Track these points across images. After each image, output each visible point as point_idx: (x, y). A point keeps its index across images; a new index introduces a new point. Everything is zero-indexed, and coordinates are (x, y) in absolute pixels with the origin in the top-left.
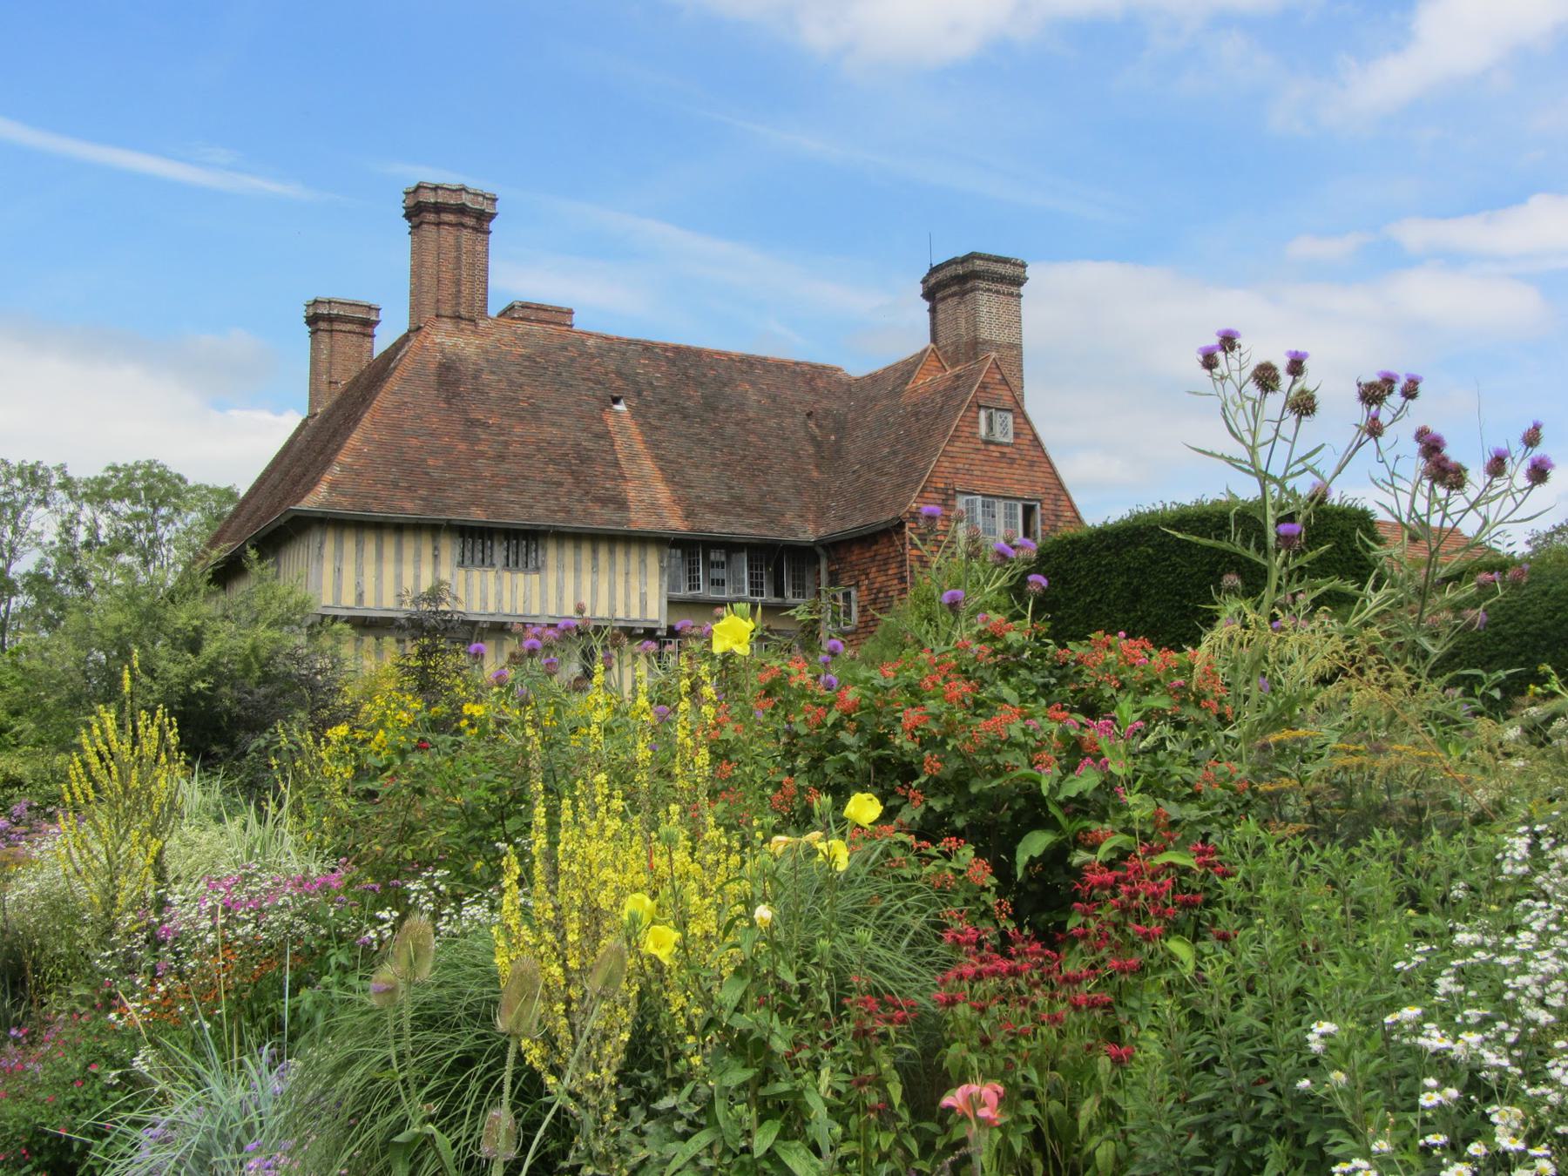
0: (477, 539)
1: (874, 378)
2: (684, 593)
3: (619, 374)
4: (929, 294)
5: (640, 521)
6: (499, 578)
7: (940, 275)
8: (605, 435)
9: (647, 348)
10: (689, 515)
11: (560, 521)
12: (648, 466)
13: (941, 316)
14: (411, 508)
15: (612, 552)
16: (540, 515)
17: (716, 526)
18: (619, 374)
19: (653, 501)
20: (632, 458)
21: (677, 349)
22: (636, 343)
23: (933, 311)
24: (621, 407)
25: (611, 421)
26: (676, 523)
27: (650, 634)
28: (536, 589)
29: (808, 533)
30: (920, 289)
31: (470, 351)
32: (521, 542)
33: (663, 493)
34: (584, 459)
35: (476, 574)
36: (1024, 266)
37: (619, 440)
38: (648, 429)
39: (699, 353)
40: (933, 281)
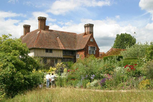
0: (47, 50)
1: (80, 35)
2: (64, 55)
3: (57, 34)
4: (85, 27)
5: (61, 48)
6: (49, 54)
7: (86, 25)
8: (57, 40)
9: (59, 31)
10: (65, 48)
11: (54, 48)
12: (61, 43)
13: (86, 29)
14: (42, 47)
15: (58, 51)
16: (52, 47)
17: (67, 49)
18: (57, 34)
19: (62, 47)
20: (59, 42)
21: (62, 32)
22: (58, 31)
23: (85, 28)
24: (58, 37)
25: (57, 39)
26: (64, 49)
27: (61, 58)
28: (52, 54)
29: (75, 49)
30: (84, 26)
31: (45, 32)
32: (51, 51)
33: (62, 46)
34: (56, 43)
35: (47, 53)
36: (93, 25)
37: (58, 41)
38: (61, 40)
39: (64, 32)
40: (85, 26)
